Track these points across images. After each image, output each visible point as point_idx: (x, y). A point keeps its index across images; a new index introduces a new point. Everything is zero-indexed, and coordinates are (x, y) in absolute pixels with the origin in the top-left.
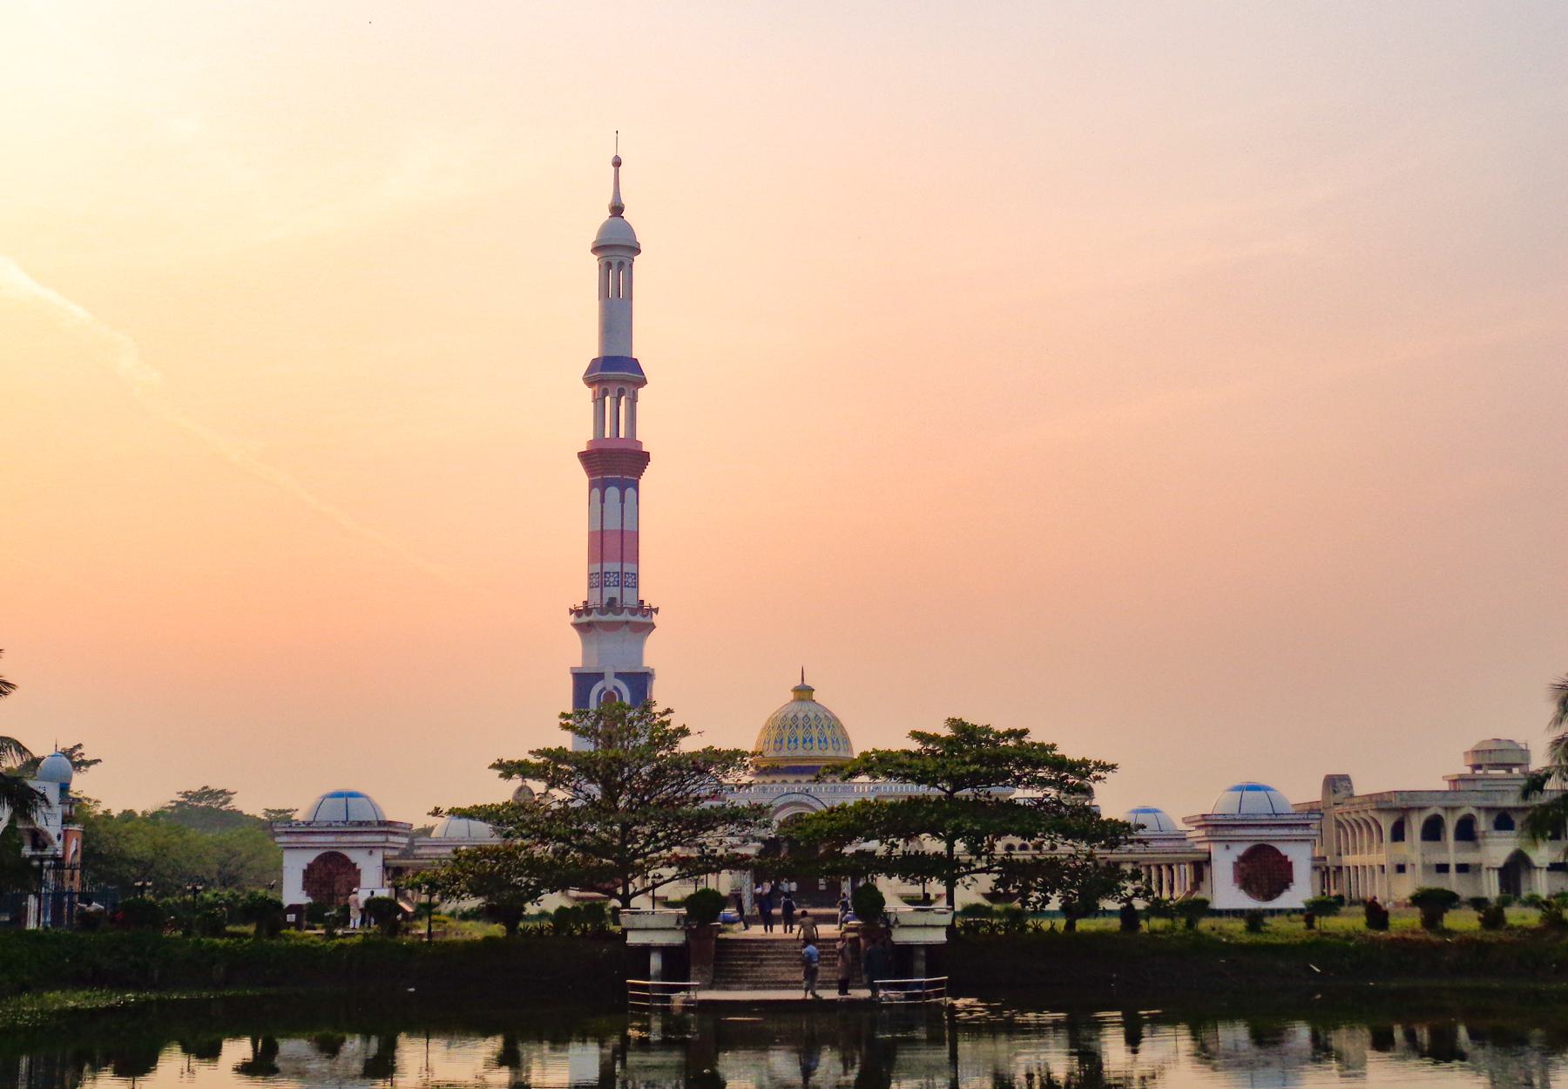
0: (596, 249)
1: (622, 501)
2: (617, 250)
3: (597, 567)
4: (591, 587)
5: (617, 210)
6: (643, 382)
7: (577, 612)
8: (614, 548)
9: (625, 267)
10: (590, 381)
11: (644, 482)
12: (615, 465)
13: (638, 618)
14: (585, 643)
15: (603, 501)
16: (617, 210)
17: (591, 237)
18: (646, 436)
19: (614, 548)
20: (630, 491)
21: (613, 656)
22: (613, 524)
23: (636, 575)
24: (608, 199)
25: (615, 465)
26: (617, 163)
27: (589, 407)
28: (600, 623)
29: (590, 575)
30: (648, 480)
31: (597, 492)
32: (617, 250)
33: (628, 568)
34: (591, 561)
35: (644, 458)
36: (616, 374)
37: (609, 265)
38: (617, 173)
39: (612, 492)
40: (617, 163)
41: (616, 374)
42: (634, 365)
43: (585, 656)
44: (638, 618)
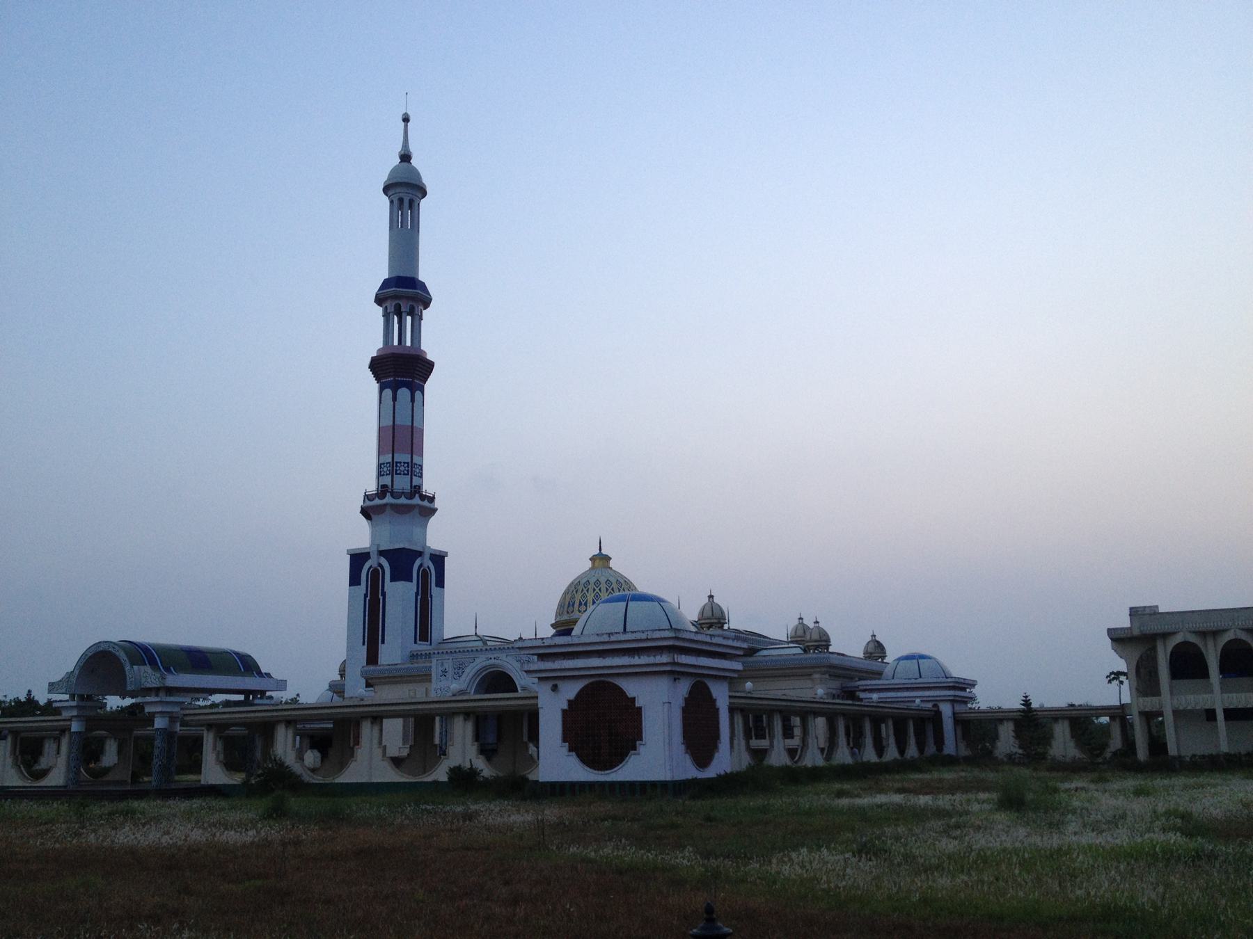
0: (386, 190)
1: (413, 400)
2: (405, 191)
3: (388, 458)
4: (380, 474)
5: (406, 157)
6: (426, 302)
7: (367, 497)
8: (401, 444)
9: (413, 206)
10: (379, 300)
11: (428, 386)
12: (402, 371)
13: (426, 503)
14: (372, 526)
15: (394, 399)
16: (406, 157)
17: (383, 178)
18: (430, 348)
19: (401, 444)
20: (418, 393)
21: (395, 535)
22: (403, 419)
23: (421, 466)
24: (398, 148)
25: (402, 371)
26: (406, 120)
27: (382, 319)
28: (392, 505)
29: (380, 466)
30: (432, 386)
31: (388, 393)
32: (405, 191)
33: (416, 459)
34: (380, 452)
35: (430, 365)
36: (404, 295)
37: (401, 200)
38: (406, 127)
39: (404, 393)
40: (406, 120)
41: (404, 295)
42: (423, 286)
43: (373, 536)
44: (426, 503)
